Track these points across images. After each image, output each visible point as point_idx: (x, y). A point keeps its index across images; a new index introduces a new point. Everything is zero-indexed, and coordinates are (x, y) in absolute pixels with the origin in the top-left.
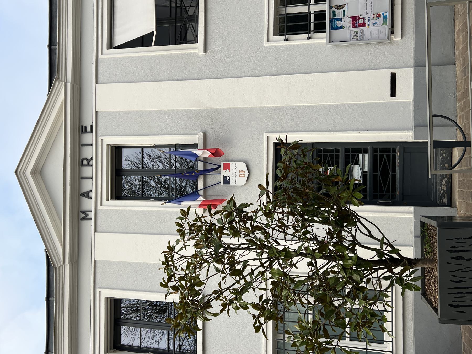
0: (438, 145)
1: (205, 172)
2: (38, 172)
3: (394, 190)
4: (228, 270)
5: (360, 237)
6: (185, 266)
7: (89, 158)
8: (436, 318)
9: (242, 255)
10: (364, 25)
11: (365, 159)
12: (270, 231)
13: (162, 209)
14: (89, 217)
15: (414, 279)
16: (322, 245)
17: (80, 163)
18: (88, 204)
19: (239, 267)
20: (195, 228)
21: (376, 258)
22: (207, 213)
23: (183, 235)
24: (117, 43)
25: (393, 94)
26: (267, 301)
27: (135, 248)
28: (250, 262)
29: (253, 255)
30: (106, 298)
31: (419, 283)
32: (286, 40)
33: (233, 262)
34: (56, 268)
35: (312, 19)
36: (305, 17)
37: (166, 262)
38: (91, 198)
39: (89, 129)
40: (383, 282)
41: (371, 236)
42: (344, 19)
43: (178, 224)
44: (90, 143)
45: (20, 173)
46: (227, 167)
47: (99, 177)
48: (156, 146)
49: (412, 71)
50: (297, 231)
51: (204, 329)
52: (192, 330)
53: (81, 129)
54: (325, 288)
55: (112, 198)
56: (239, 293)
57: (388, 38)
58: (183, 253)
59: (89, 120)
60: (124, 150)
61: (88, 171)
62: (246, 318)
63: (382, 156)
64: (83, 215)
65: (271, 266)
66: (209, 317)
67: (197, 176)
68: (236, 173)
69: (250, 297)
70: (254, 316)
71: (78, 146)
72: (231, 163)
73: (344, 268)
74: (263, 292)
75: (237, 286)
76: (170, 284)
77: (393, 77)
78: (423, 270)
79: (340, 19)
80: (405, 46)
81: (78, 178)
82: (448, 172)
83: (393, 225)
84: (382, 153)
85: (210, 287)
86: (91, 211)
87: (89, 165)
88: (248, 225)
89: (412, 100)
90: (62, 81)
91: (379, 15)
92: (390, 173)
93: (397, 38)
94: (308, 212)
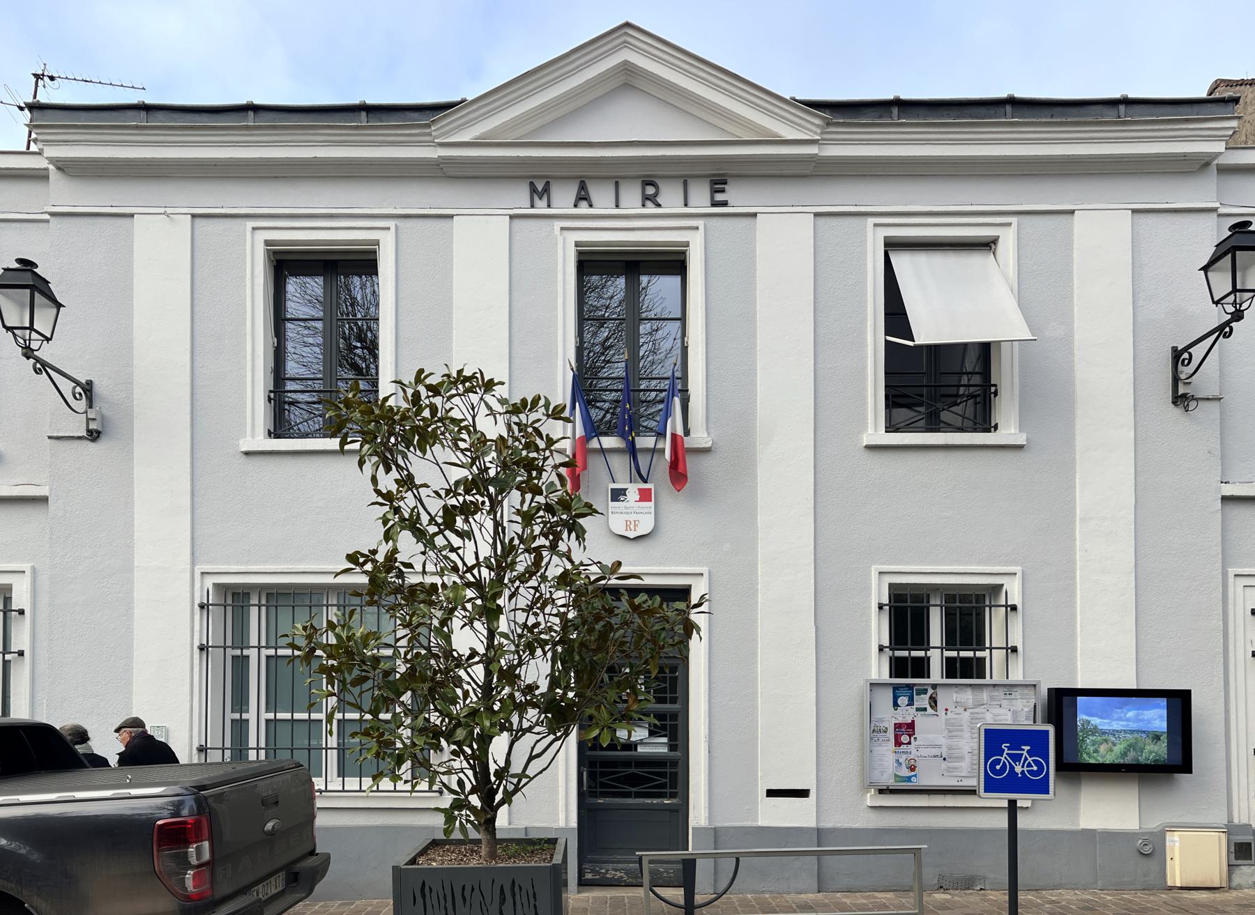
0: (689, 866)
1: (632, 451)
2: (629, 80)
3: (604, 795)
4: (453, 502)
5: (529, 739)
6: (455, 414)
7: (659, 200)
8: (402, 860)
9: (483, 524)
10: (898, 743)
11: (658, 747)
12: (533, 583)
13: (560, 363)
14: (538, 202)
15: (463, 829)
16: (510, 676)
17: (649, 178)
18: (563, 198)
19: (459, 522)
20: (531, 435)
21: (493, 768)
22: (559, 459)
23: (516, 410)
24: (898, 260)
25: (771, 793)
26: (401, 575)
27: (479, 303)
28: (470, 545)
29: (485, 551)
30: (377, 243)
31: (457, 835)
32: (881, 607)
33: (468, 510)
34: (428, 126)
35: (915, 654)
36: (921, 640)
37: (461, 378)
38: (576, 206)
39: (719, 197)
40: (454, 778)
41: (531, 758)
42: (912, 710)
43: (536, 400)
44: (691, 202)
45: (626, 34)
46: (645, 496)
47: (625, 223)
48: (685, 349)
49: (813, 824)
50: (531, 630)
51: (342, 451)
52: (335, 428)
53: (719, 179)
54: (432, 677)
55: (580, 253)
56: (412, 524)
57: (871, 785)
58: (483, 410)
59: (738, 197)
60: (678, 279)
61: (631, 199)
62: (370, 537)
63: (663, 775)
64: (540, 188)
65: (469, 585)
66: (368, 467)
67: (623, 435)
68: (630, 515)
69: (408, 546)
70: (374, 552)
71: (686, 173)
72: (652, 504)
73: (474, 713)
74: (419, 568)
75: (425, 519)
76: (422, 389)
77: (803, 793)
78: (477, 842)
79: (911, 703)
80: (856, 812)
81: (615, 174)
82: (646, 879)
83: (549, 799)
84: (668, 777)
85: (420, 467)
86: (549, 206)
87: (646, 198)
88: (542, 541)
89: (760, 823)
90: (822, 133)
91: (912, 769)
92: (634, 790)
93: (871, 799)
94: (569, 651)
